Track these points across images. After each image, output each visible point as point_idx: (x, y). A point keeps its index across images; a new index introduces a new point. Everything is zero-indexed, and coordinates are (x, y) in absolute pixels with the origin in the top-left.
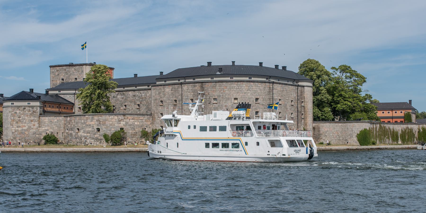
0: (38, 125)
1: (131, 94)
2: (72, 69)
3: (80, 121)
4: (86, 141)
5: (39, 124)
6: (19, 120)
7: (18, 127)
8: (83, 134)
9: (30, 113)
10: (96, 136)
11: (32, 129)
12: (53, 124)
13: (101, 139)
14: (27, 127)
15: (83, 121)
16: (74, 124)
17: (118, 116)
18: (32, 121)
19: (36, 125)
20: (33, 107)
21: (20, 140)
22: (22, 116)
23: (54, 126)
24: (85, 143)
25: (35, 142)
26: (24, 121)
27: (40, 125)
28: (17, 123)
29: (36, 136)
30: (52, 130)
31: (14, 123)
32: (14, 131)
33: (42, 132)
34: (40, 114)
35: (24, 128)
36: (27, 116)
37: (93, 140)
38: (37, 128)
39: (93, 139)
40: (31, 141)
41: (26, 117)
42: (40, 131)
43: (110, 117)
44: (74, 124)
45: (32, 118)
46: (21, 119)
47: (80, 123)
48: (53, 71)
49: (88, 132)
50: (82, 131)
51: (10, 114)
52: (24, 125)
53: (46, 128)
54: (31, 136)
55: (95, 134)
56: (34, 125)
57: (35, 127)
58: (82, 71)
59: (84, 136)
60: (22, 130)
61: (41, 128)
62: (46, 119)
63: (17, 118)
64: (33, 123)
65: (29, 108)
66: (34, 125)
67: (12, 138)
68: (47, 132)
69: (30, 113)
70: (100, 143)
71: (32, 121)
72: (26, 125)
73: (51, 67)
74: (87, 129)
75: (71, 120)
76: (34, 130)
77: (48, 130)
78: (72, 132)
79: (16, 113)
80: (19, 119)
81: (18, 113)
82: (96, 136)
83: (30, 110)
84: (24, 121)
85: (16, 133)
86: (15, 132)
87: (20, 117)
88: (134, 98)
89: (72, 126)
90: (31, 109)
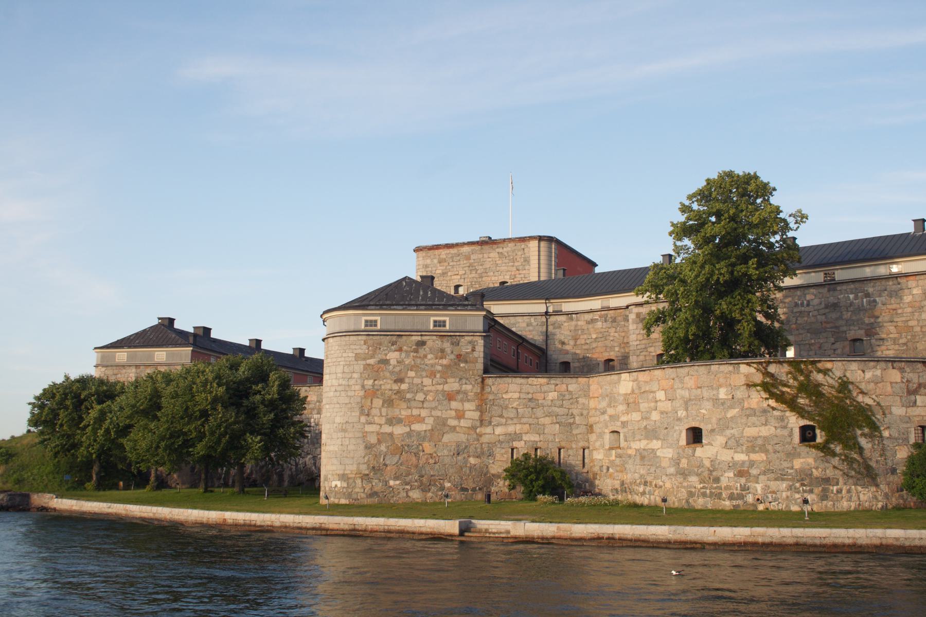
0: (476, 415)
1: (816, 301)
2: (492, 254)
3: (706, 393)
4: (744, 488)
5: (481, 409)
6: (398, 392)
7: (390, 422)
8: (726, 456)
9: (445, 362)
10: (798, 463)
11: (453, 429)
12: (539, 412)
13: (827, 480)
14: (430, 421)
15: (723, 394)
16: (667, 406)
17: (902, 370)
18: (450, 397)
19: (468, 414)
20: (454, 336)
21: (396, 478)
22: (411, 374)
23: (547, 420)
24: (741, 497)
25: (464, 490)
26: (420, 397)
27: (486, 417)
28: (389, 403)
29: (466, 460)
30: (534, 438)
31: (378, 402)
32: (373, 439)
33: (492, 445)
34: (486, 371)
35: (417, 427)
36: (432, 375)
37: (784, 485)
38: (474, 428)
39: (781, 477)
40: (448, 485)
41: (427, 381)
42: (485, 439)
43: (869, 375)
44: (667, 406)
45: (453, 385)
46: (404, 387)
47: (708, 405)
48: (428, 261)
49: (753, 446)
50: (720, 440)
51: (359, 366)
52: (415, 412)
53: (511, 429)
54: (447, 460)
55: (792, 455)
56: (460, 415)
57: (463, 423)
58: (527, 261)
59: (732, 465)
60: (409, 434)
61: (489, 430)
62: (511, 389)
63: (388, 385)
64: (454, 404)
65: (438, 343)
66: (460, 415)
67: (364, 469)
68: (515, 444)
69: (445, 362)
70: (824, 497)
71: (450, 397)
72: (424, 413)
73: (418, 250)
74: (751, 432)
75: (641, 392)
76: (462, 438)
77: (517, 437)
78: (655, 444)
79: (386, 362)
80: (395, 387)
81: (393, 362)
82: (798, 463)
83: (442, 351)
84: (420, 397)
85: (383, 448)
86: (379, 442)
87: (400, 381)
88: (834, 315)
89: (655, 416)
90: (447, 346)
